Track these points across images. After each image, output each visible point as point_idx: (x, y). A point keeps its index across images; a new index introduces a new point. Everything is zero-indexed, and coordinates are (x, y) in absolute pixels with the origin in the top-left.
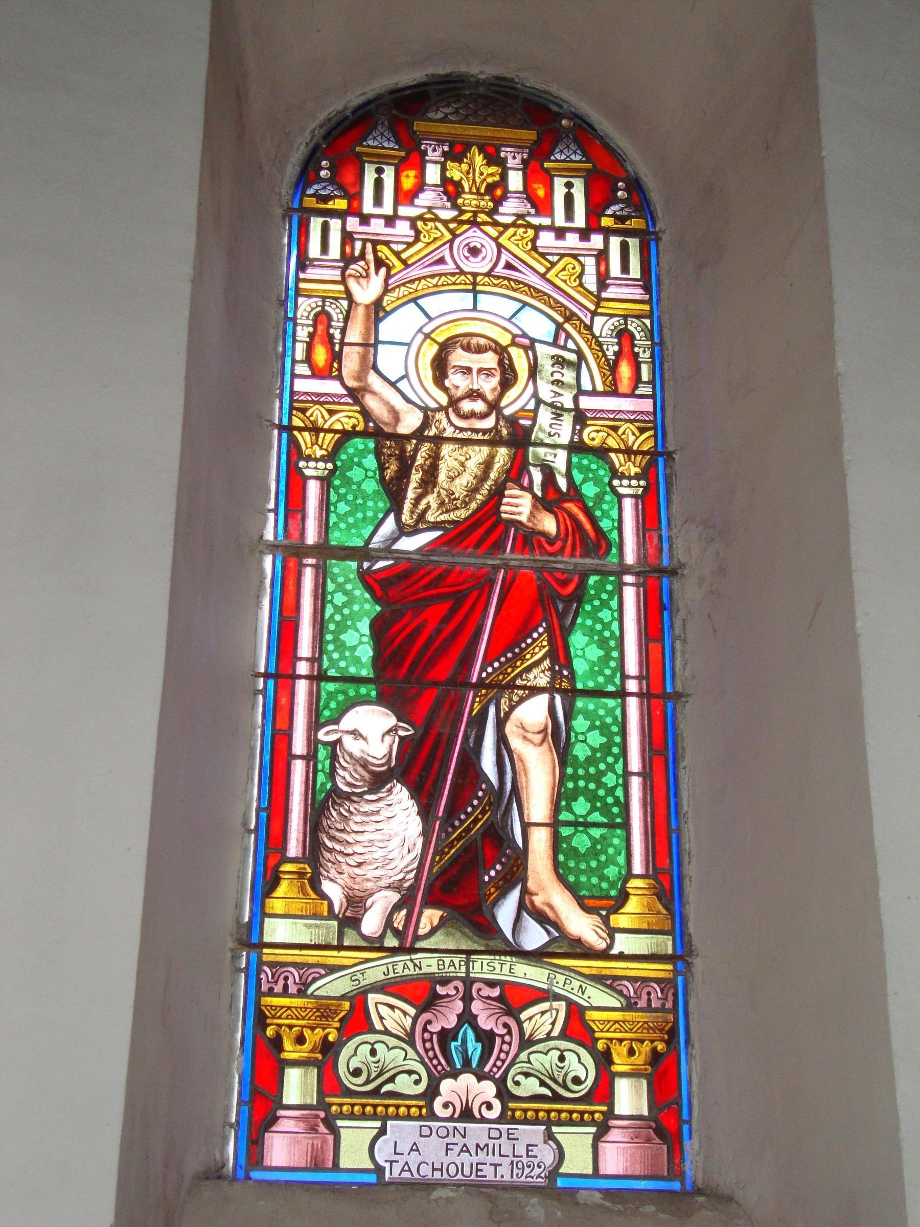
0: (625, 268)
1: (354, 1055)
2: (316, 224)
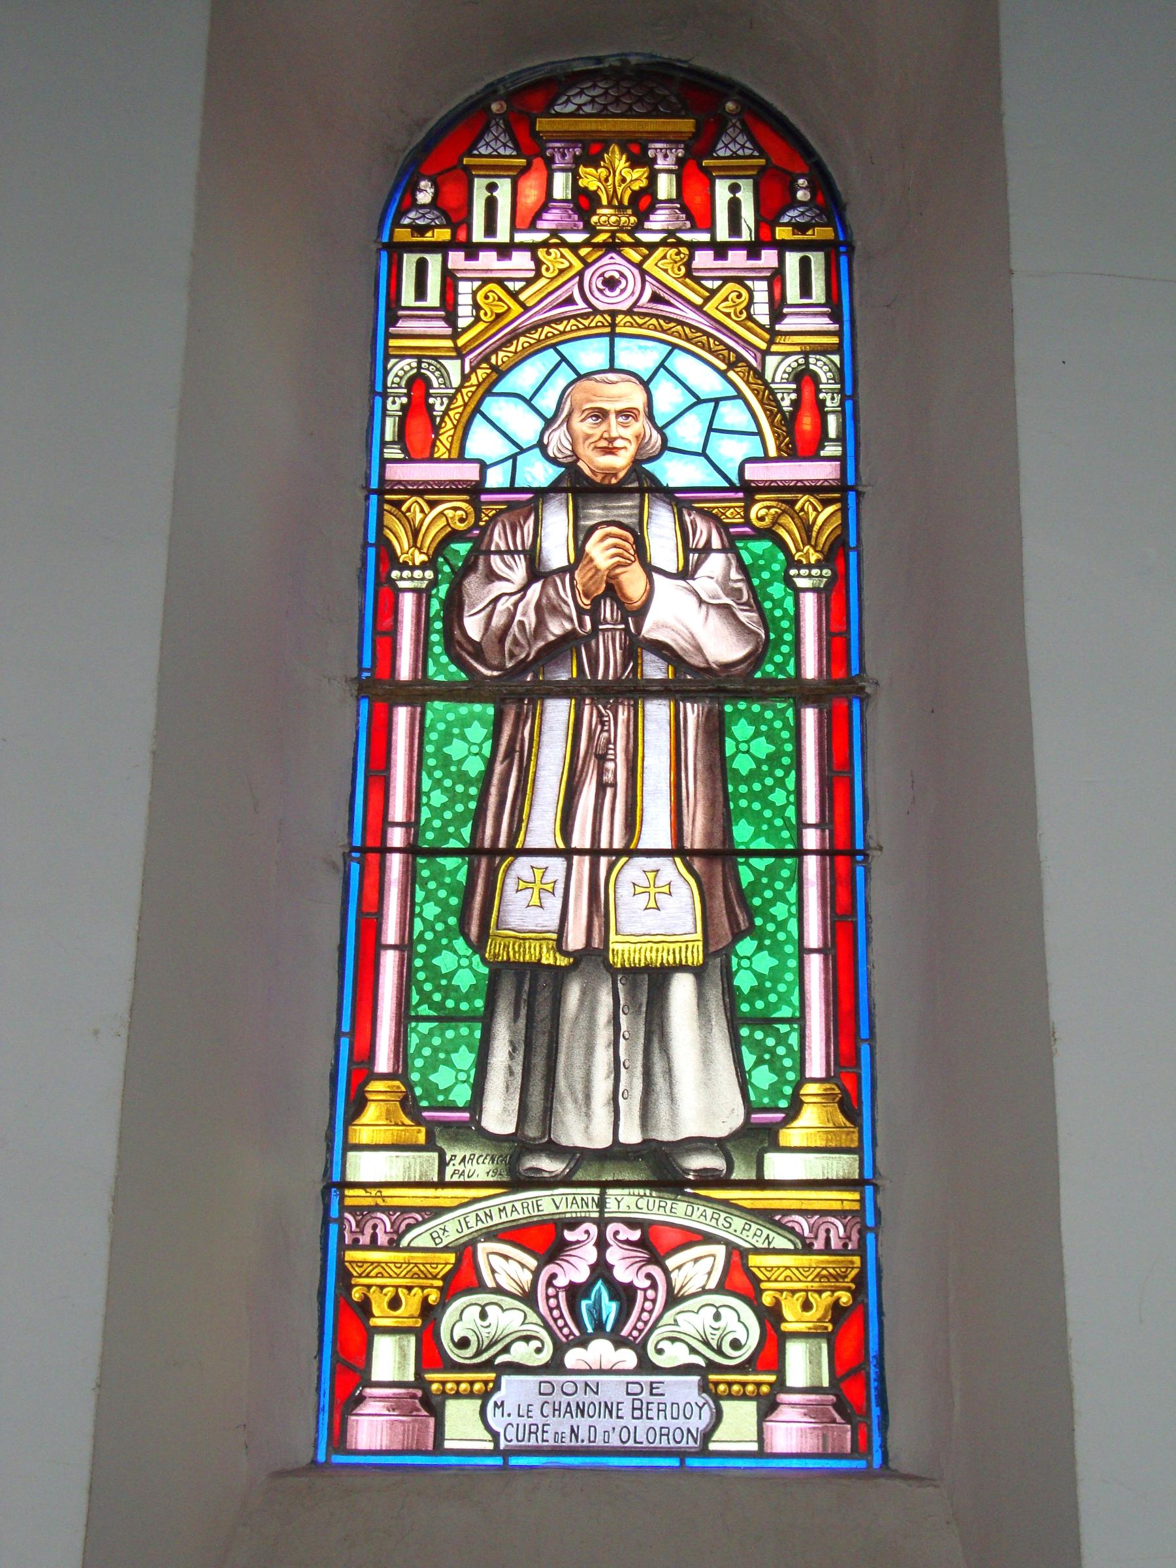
0: (806, 290)
1: (461, 1320)
2: (409, 262)
